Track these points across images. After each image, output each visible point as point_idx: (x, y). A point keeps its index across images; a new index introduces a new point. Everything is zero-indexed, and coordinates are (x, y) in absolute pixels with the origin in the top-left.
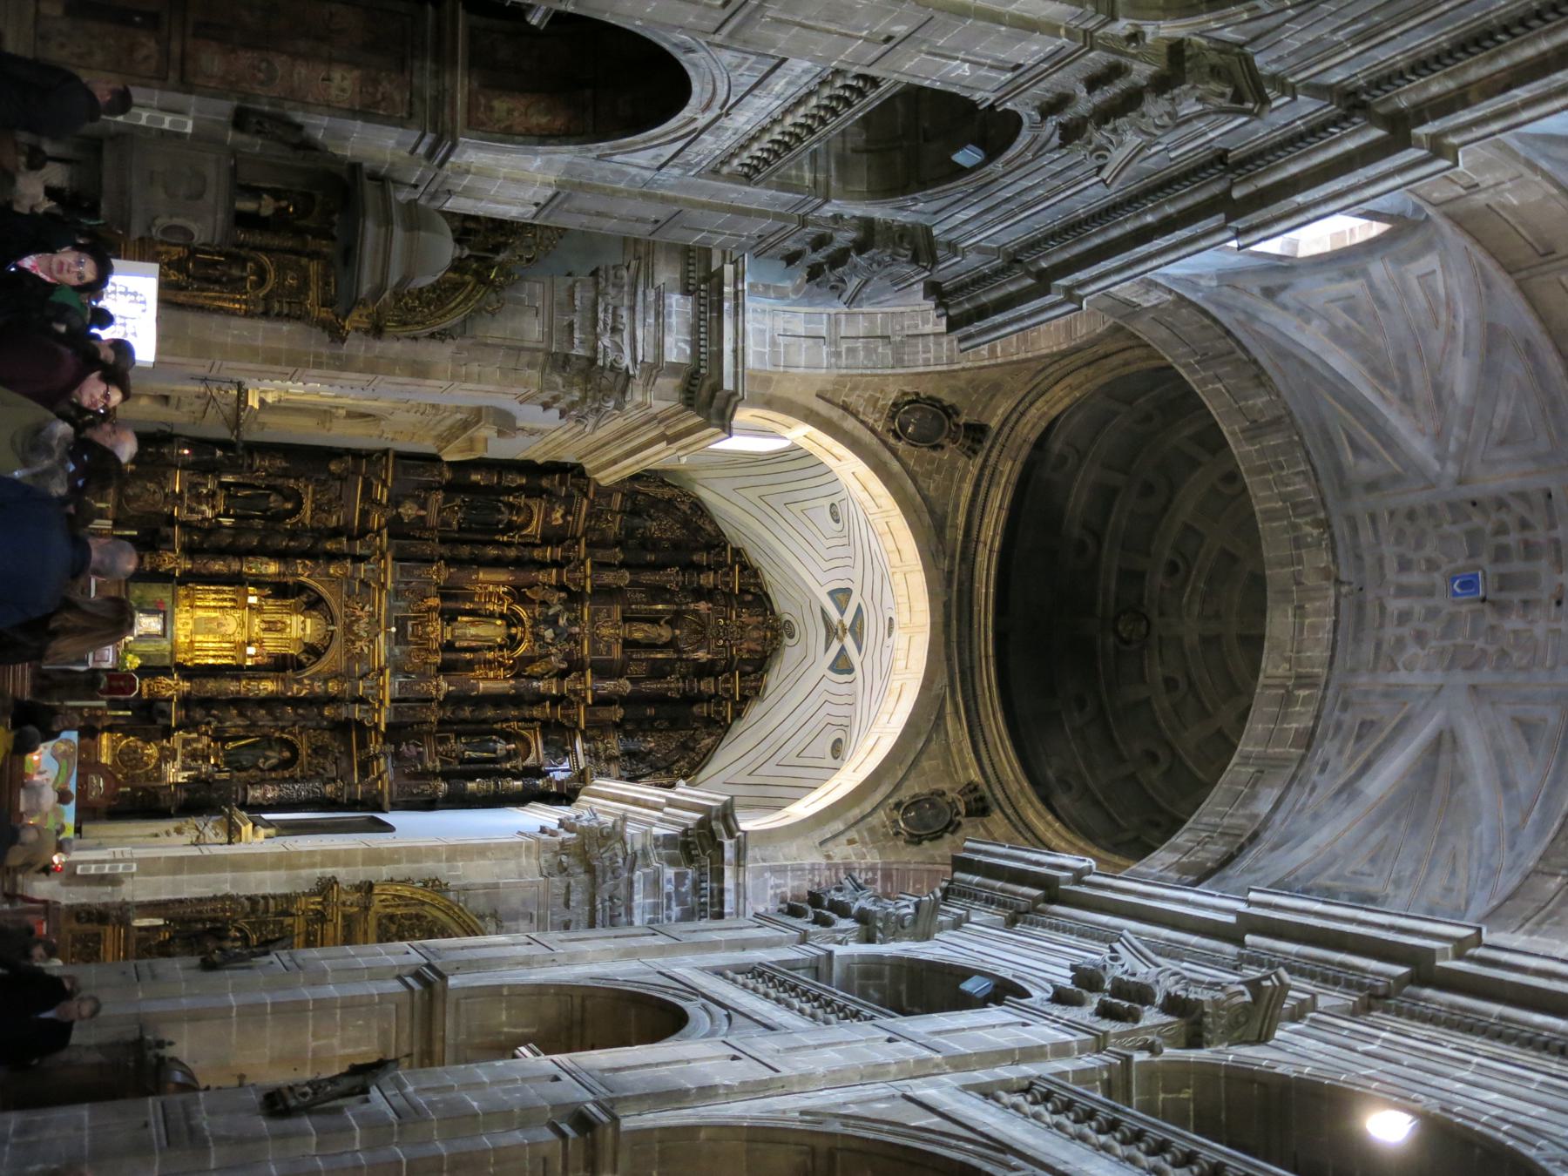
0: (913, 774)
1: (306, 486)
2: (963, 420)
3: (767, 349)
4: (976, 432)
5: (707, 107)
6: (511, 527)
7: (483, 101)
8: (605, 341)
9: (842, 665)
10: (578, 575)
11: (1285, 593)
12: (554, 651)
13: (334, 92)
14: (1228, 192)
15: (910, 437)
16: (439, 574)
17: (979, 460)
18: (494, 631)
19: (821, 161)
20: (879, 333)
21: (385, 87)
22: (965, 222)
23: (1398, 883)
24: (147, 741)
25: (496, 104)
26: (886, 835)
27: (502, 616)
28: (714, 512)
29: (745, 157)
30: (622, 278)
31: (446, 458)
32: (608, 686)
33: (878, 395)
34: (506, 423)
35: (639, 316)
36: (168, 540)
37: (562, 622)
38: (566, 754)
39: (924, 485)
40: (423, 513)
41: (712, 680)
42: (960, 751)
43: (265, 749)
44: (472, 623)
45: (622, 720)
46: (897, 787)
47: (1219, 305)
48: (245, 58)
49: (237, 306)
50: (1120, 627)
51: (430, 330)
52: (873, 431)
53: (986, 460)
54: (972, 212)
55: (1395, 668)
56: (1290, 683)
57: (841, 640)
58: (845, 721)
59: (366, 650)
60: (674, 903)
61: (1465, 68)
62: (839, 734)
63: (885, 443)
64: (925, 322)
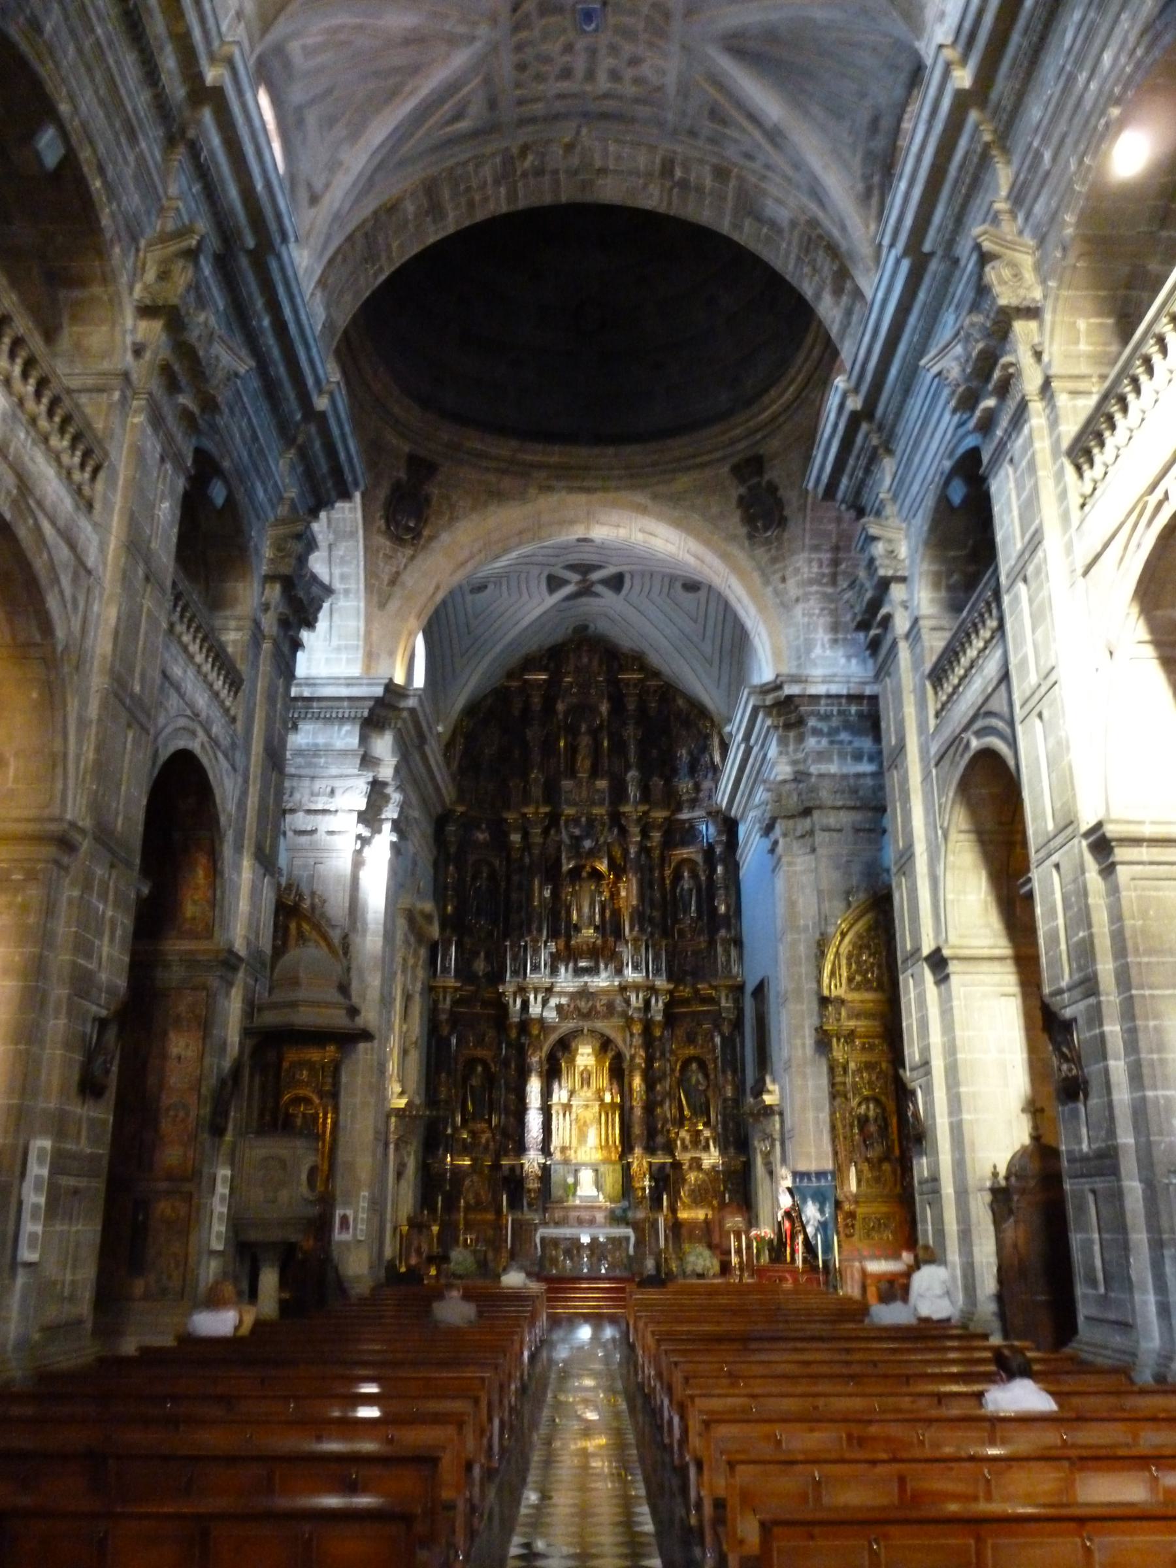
3: (344, 656)
6: (492, 877)
7: (187, 926)
9: (616, 582)
11: (585, 186)
12: (602, 840)
13: (189, 1053)
14: (250, 253)
21: (182, 1008)
22: (265, 491)
23: (863, 95)
24: (684, 1180)
25: (189, 914)
26: (778, 548)
29: (224, 693)
32: (633, 791)
36: (512, 1168)
37: (577, 832)
44: (579, 911)
45: (661, 776)
47: (325, 247)
48: (166, 1126)
52: (412, 558)
54: (258, 485)
55: (659, 89)
56: (668, 184)
57: (593, 583)
58: (667, 580)
62: (678, 585)
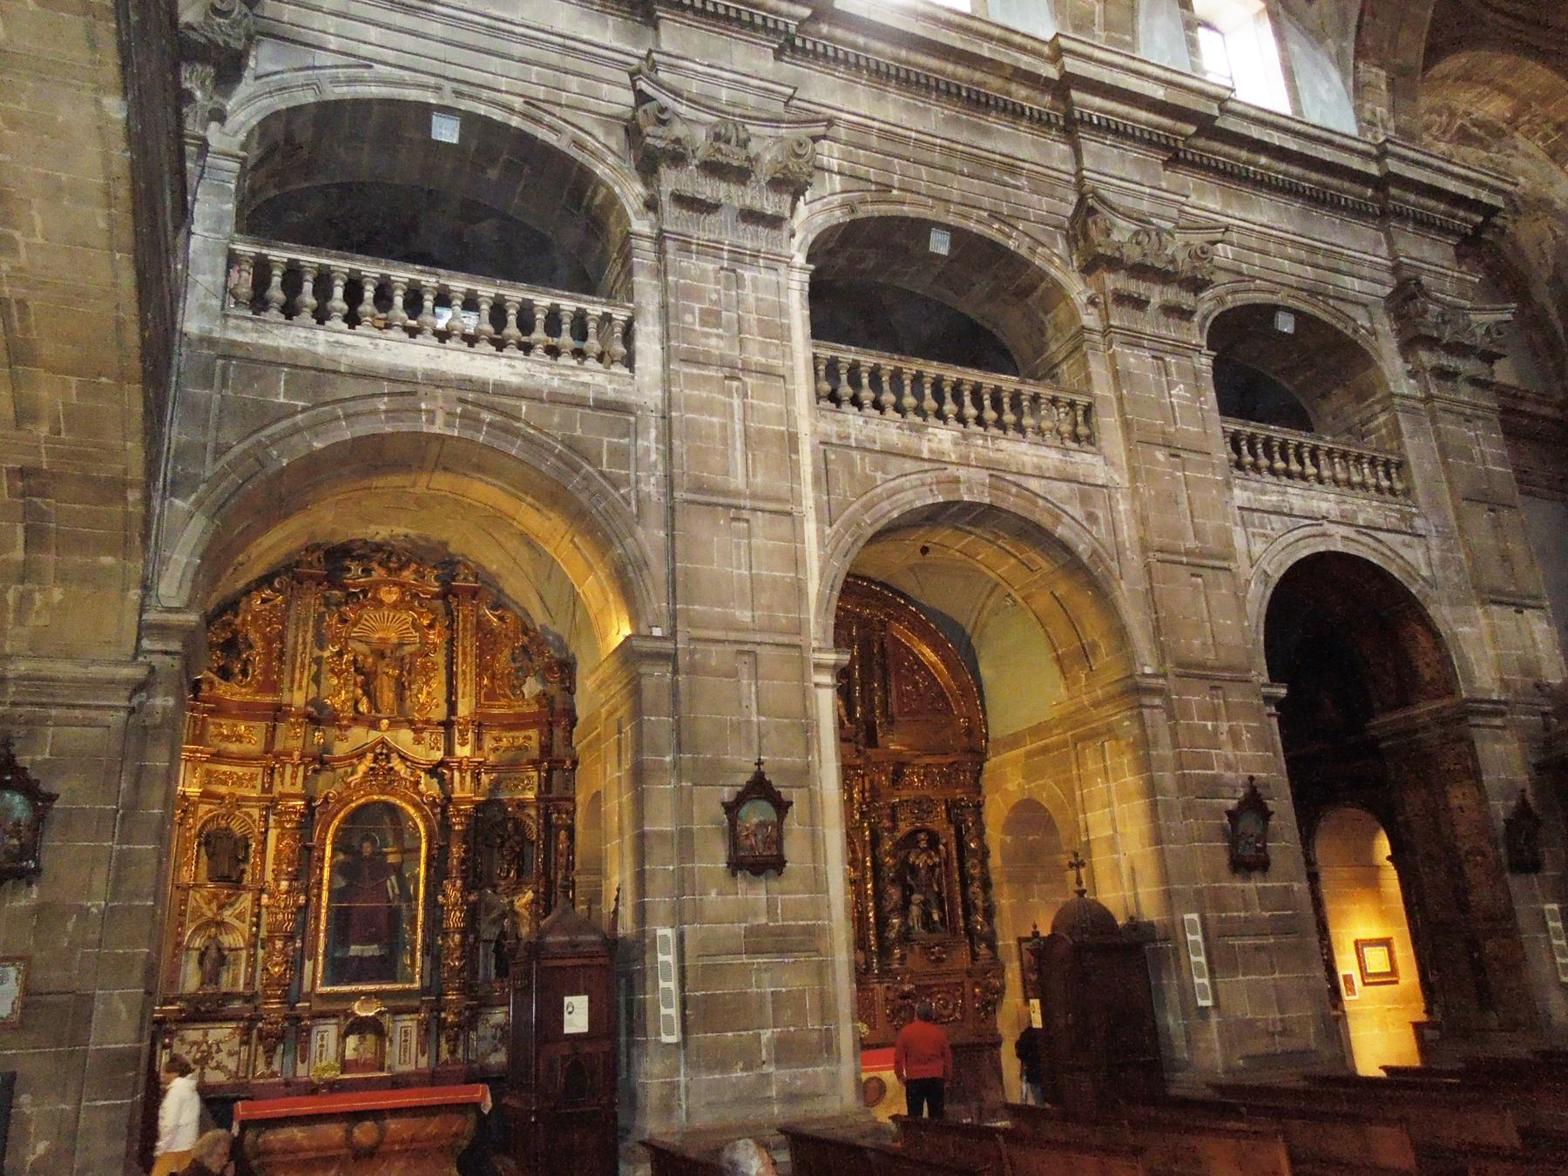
5: (1324, 535)
13: (1469, 802)
19: (1367, 414)
25: (1427, 678)
54: (1348, 281)
61: (998, 90)
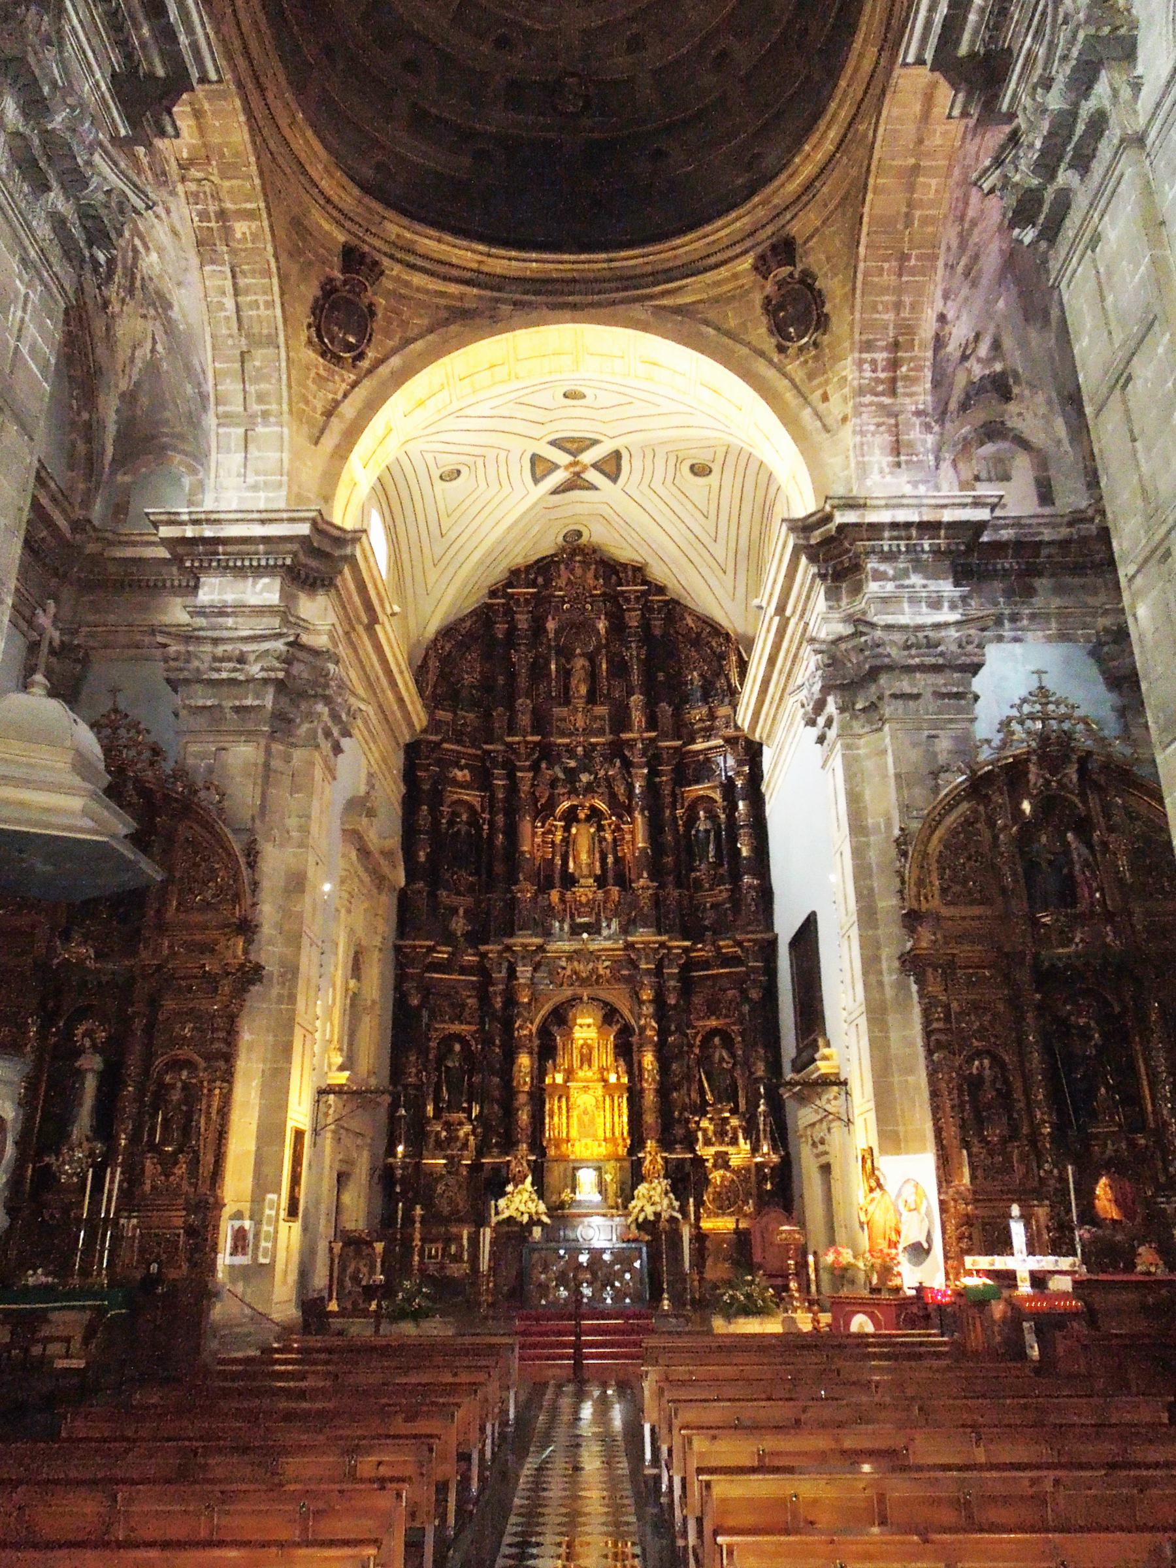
0: (747, 338)
1: (436, 1030)
2: (338, 275)
4: (352, 258)
6: (474, 822)
8: (255, 670)
9: (612, 466)
10: (522, 750)
12: (602, 773)
15: (360, 341)
16: (526, 891)
17: (386, 262)
18: (583, 834)
20: (237, 366)
24: (707, 1181)
26: (816, 358)
27: (567, 829)
28: (452, 618)
30: (178, 652)
31: (403, 884)
32: (637, 717)
33: (312, 375)
34: (359, 806)
35: (226, 634)
36: (496, 1168)
38: (708, 760)
39: (416, 331)
40: (461, 911)
41: (627, 614)
42: (717, 284)
43: (712, 1063)
46: (762, 354)
49: (217, 1091)
50: (571, 109)
51: (243, 867)
52: (354, 385)
53: (385, 254)
59: (607, 963)
60: (907, 582)
62: (685, 468)
63: (370, 371)
64: (221, 306)
